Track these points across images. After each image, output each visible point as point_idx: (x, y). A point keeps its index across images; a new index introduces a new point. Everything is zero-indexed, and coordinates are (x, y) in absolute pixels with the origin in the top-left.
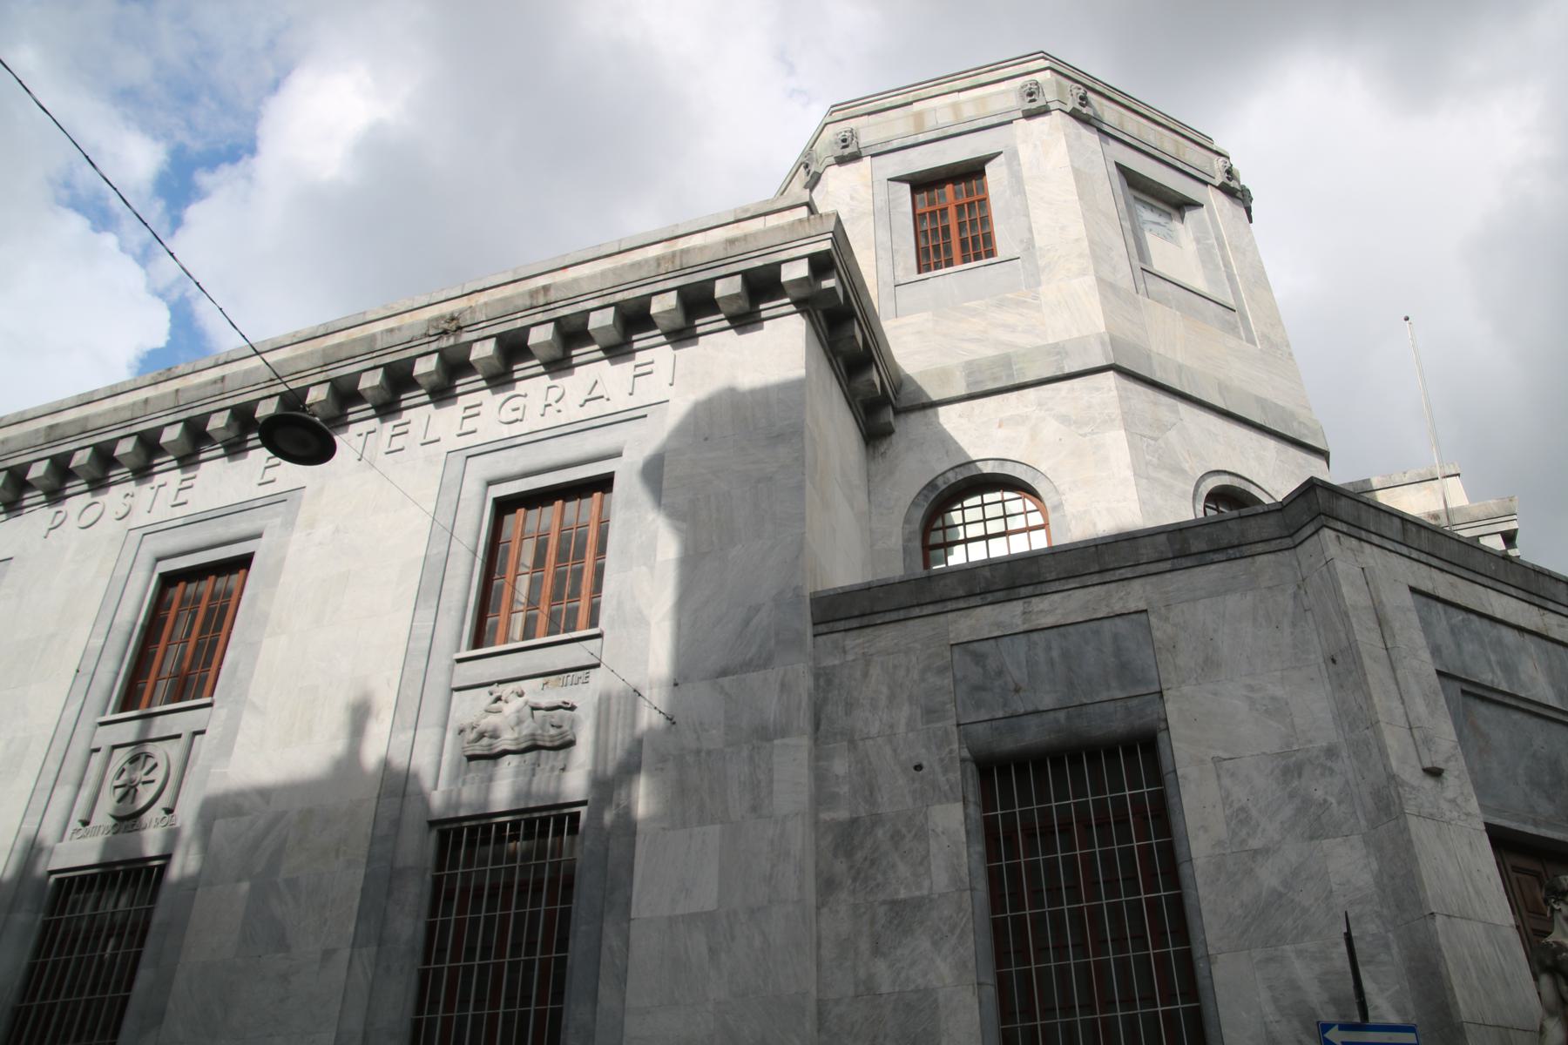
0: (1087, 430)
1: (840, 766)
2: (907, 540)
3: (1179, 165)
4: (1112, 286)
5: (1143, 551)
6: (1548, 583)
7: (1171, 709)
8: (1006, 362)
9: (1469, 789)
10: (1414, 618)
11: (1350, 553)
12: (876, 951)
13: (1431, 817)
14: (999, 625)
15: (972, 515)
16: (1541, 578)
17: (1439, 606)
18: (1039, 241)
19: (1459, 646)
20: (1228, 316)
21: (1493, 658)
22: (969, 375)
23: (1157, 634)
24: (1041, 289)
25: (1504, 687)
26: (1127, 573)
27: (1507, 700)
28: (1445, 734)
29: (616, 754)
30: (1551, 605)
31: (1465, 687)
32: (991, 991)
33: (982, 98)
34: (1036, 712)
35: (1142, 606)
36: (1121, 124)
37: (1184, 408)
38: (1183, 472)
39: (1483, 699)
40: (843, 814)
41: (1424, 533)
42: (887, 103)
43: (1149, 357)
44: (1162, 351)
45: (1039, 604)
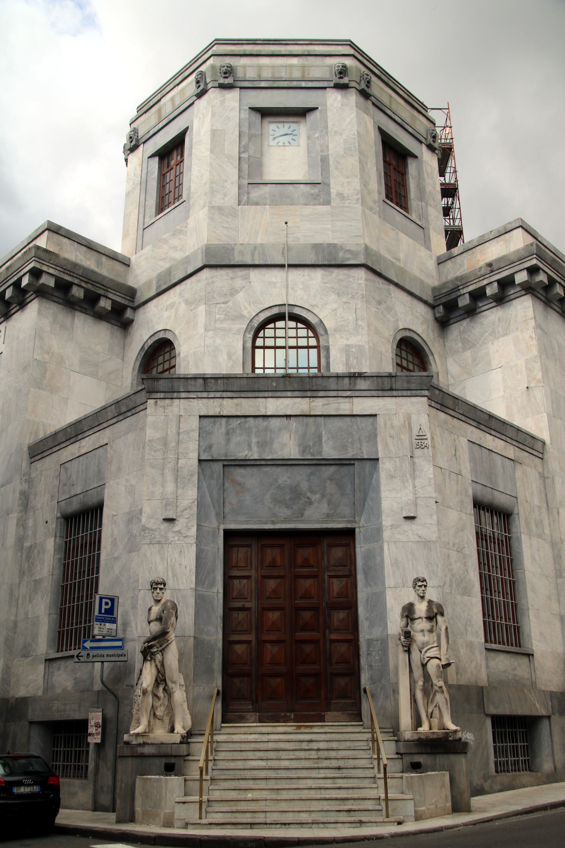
0: (193, 307)
1: (30, 523)
2: (133, 380)
3: (303, 84)
4: (220, 209)
5: (109, 414)
6: (320, 381)
7: (106, 491)
8: (169, 272)
10: (196, 435)
11: (161, 409)
12: (30, 601)
13: (159, 543)
14: (72, 454)
15: (161, 359)
16: (314, 380)
17: (224, 420)
18: (192, 190)
20: (315, 190)
21: (254, 440)
22: (157, 283)
23: (109, 455)
24: (189, 220)
25: (256, 457)
26: (105, 425)
28: (190, 494)
30: (322, 394)
31: (226, 463)
32: (55, 616)
33: (183, 90)
34: (76, 495)
36: (259, 76)
37: (254, 274)
38: (243, 317)
40: (27, 544)
42: (151, 104)
43: (233, 249)
44: (246, 241)
45: (83, 442)
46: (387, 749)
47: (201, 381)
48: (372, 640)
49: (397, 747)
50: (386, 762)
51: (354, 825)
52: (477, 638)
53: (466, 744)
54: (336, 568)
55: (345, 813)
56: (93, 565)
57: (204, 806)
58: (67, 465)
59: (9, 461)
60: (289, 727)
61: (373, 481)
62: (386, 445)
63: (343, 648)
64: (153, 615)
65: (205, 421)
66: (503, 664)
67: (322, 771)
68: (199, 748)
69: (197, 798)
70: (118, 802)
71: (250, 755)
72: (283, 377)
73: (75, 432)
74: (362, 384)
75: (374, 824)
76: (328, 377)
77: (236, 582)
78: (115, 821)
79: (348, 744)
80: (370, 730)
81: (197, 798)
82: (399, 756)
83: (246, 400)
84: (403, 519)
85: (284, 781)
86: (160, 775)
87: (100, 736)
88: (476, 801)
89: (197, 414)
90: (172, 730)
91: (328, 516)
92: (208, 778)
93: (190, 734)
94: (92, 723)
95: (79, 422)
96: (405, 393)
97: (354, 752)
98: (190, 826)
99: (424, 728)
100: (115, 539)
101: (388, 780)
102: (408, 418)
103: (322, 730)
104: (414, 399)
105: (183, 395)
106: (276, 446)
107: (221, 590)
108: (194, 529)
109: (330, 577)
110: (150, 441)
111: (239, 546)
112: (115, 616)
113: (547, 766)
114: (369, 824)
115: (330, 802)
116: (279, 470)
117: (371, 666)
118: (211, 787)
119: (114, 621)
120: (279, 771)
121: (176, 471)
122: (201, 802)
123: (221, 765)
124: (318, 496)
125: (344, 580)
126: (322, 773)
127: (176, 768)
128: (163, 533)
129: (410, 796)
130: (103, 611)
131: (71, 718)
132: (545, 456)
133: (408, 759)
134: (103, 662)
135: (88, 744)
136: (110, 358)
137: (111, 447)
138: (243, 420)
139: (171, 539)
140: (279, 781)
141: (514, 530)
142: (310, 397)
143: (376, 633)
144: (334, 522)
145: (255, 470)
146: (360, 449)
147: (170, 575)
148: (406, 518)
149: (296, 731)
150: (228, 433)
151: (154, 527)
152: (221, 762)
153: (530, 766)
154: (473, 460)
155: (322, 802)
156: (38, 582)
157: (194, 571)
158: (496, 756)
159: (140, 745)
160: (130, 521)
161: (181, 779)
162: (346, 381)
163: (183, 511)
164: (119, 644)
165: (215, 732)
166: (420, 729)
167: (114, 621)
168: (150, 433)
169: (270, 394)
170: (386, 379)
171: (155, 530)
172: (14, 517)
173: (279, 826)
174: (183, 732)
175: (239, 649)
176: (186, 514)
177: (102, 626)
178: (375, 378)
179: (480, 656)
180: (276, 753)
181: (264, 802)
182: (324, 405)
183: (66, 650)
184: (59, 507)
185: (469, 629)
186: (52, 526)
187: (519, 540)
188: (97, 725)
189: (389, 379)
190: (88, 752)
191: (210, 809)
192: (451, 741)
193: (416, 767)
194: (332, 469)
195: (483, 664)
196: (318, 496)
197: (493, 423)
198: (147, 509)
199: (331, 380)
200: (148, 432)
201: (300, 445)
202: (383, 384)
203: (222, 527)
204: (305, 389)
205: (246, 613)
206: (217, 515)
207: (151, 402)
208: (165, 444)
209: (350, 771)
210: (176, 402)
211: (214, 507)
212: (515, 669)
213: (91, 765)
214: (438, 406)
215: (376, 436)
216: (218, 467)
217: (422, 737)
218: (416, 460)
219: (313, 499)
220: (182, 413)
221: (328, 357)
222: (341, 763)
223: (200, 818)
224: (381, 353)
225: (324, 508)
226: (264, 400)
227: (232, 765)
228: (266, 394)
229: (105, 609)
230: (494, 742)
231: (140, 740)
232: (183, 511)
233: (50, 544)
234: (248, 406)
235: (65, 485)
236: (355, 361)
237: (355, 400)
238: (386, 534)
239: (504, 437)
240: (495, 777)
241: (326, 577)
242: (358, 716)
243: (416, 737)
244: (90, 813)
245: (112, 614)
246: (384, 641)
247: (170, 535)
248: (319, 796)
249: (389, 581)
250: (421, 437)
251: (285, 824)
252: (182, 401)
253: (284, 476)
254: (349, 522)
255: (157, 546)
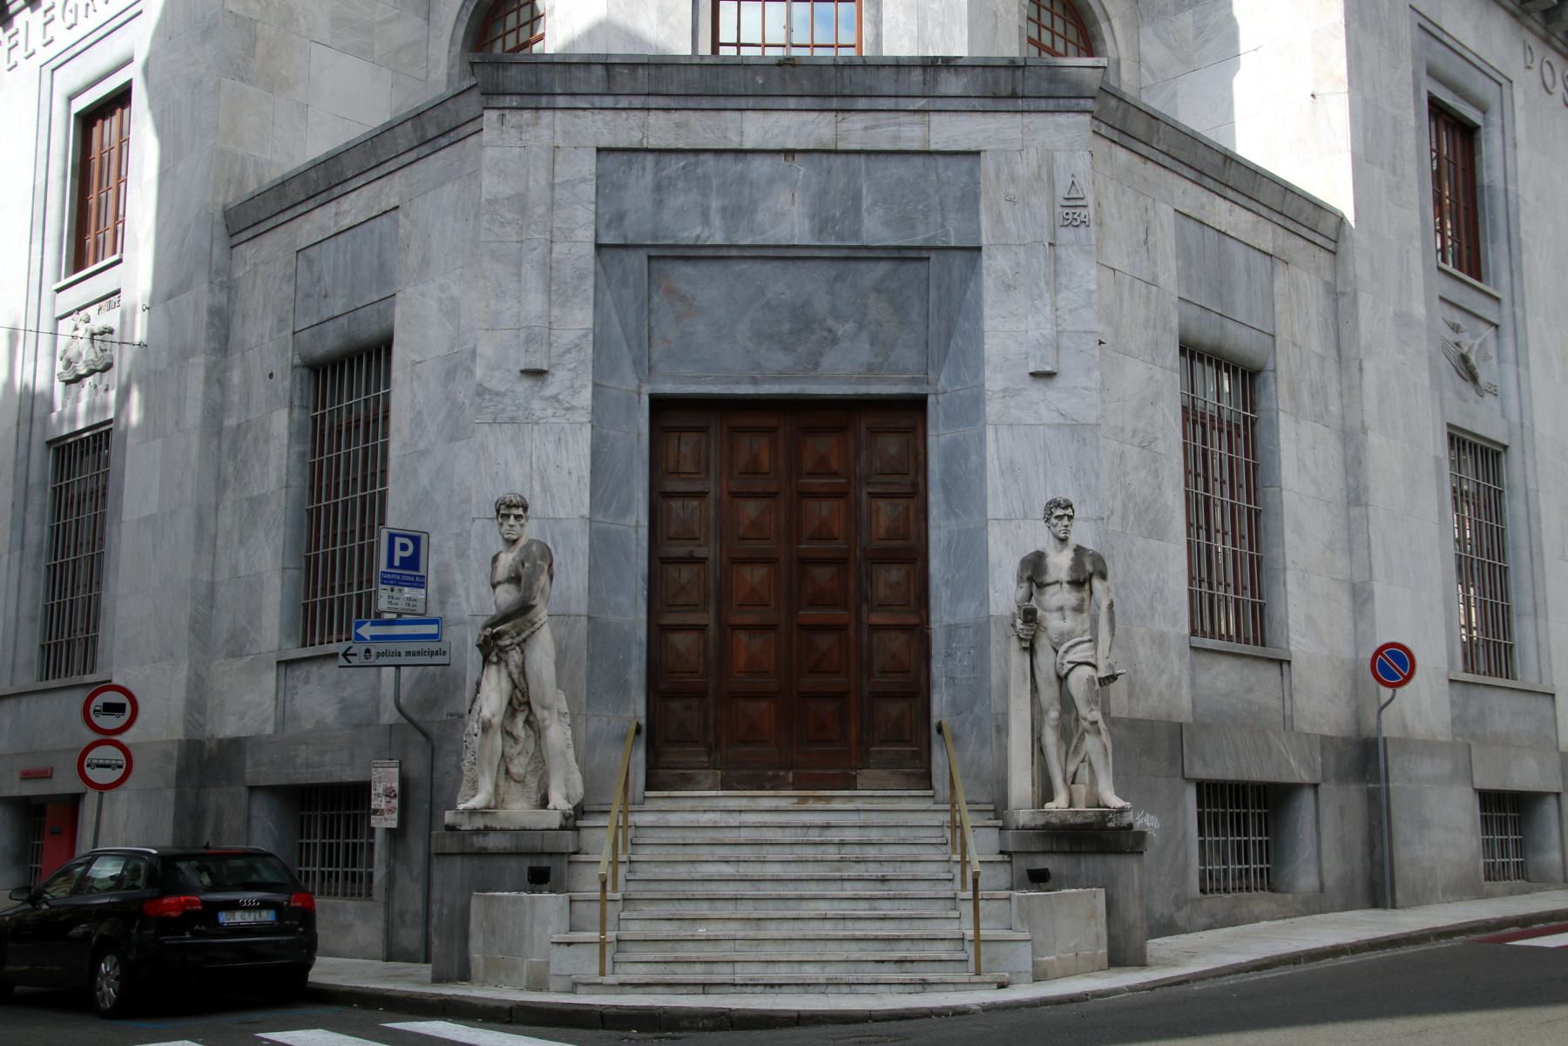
1: (236, 377)
2: (451, 67)
6: (859, 75)
7: (398, 310)
9: (587, 379)
10: (589, 190)
11: (513, 132)
12: (241, 542)
13: (512, 421)
15: (511, 21)
16: (847, 72)
17: (650, 158)
19: (659, 204)
21: (715, 204)
23: (402, 232)
25: (718, 239)
26: (391, 166)
27: (723, 253)
28: (581, 318)
29: (124, 377)
30: (862, 103)
31: (654, 252)
35: (394, 202)
39: (687, 258)
40: (231, 422)
41: (641, 72)
45: (346, 203)
46: (982, 844)
47: (599, 71)
48: (958, 626)
49: (1002, 839)
50: (977, 868)
51: (911, 989)
52: (1174, 625)
53: (1141, 836)
54: (885, 479)
55: (892, 966)
56: (375, 465)
57: (609, 950)
58: (312, 252)
59: (183, 242)
60: (783, 799)
61: (969, 295)
62: (998, 219)
63: (897, 642)
64: (503, 570)
65: (611, 161)
66: (1228, 679)
67: (848, 885)
68: (599, 839)
69: (595, 935)
70: (435, 941)
71: (704, 853)
72: (779, 65)
73: (327, 179)
74: (952, 84)
75: (951, 987)
76: (878, 66)
77: (676, 504)
78: (429, 979)
79: (903, 833)
80: (948, 807)
81: (595, 935)
82: (1006, 858)
83: (698, 114)
84: (1029, 378)
85: (771, 904)
86: (519, 891)
87: (395, 815)
88: (1157, 946)
89: (592, 144)
90: (544, 802)
91: (870, 368)
92: (618, 896)
93: (580, 811)
94: (378, 789)
95: (334, 158)
96: (1043, 104)
97: (915, 849)
98: (580, 989)
99: (1060, 803)
100: (420, 413)
101: (982, 904)
102: (1048, 160)
103: (850, 806)
104: (1062, 119)
105: (561, 101)
106: (761, 216)
107: (645, 522)
108: (587, 393)
109: (873, 496)
110: (490, 202)
111: (682, 430)
112: (422, 572)
113: (1306, 881)
114: (941, 987)
115: (863, 945)
116: (768, 268)
117: (953, 679)
118: (623, 915)
119: (420, 583)
120: (761, 885)
121: (549, 269)
122: (603, 944)
123: (644, 872)
124: (849, 327)
125: (902, 503)
126: (849, 890)
127: (552, 877)
128: (521, 401)
129: (1026, 935)
130: (397, 563)
131: (336, 780)
132: (1342, 248)
133: (1023, 864)
134: (398, 667)
135: (372, 831)
136: (398, 15)
137: (407, 216)
138: (691, 158)
139: (539, 413)
140: (762, 904)
141: (1263, 404)
142: (837, 111)
143: (966, 611)
144: (882, 381)
145: (716, 267)
146: (943, 226)
147: (537, 488)
148: (1035, 375)
149: (797, 807)
150: (658, 188)
151: (502, 388)
152: (645, 866)
153: (1270, 882)
154: (1183, 252)
155: (846, 945)
156: (256, 503)
157: (587, 480)
158: (1203, 861)
159: (478, 831)
160: (450, 375)
161: (562, 898)
162: (917, 75)
163: (563, 354)
164: (433, 629)
165: (631, 808)
166: (1048, 805)
167: (420, 583)
168: (490, 184)
169: (751, 103)
170: (1003, 72)
171: (504, 395)
172: (198, 363)
173: (760, 989)
174: (568, 807)
175: (683, 642)
176: (571, 360)
177: (395, 594)
178: (979, 70)
179: (1178, 664)
180: (756, 849)
181: (731, 944)
182: (866, 128)
183: (321, 643)
184: (296, 344)
185: (1159, 608)
186: (284, 384)
187: (1274, 425)
188: (389, 794)
189: (1010, 72)
190: (371, 846)
191: (620, 957)
192: (1112, 829)
193: (1038, 878)
194: (882, 268)
195: (1186, 678)
196: (849, 327)
197: (1232, 175)
198: (486, 350)
199: (884, 73)
200: (486, 182)
201: (812, 217)
202: (996, 83)
203: (647, 389)
204: (826, 92)
205: (696, 568)
206: (637, 363)
207: (491, 116)
208: (523, 210)
209: (905, 884)
210: (546, 116)
211: (629, 346)
212: (1250, 690)
213: (379, 872)
214: (1115, 136)
215: (976, 198)
216: (637, 260)
217: (1054, 820)
218: (1061, 251)
219: (840, 332)
220: (559, 142)
221: (878, 22)
222: (887, 870)
223: (602, 973)
224: (995, 13)
225: (863, 352)
226: (737, 114)
227: (666, 872)
228: (742, 103)
229: (402, 558)
230: (1201, 833)
231: (479, 823)
232: (563, 354)
233: (280, 423)
234: (704, 128)
235: (308, 296)
236: (937, 32)
237: (935, 118)
238: (992, 409)
239: (1254, 206)
240: (1200, 900)
241: (864, 497)
242: (924, 779)
243: (1040, 821)
244: (380, 964)
245: (417, 568)
246: (982, 627)
247: (537, 404)
248: (841, 934)
249: (996, 506)
250: (1074, 202)
251: (772, 985)
252: (559, 114)
253: (780, 284)
254: (913, 381)
255: (508, 428)
